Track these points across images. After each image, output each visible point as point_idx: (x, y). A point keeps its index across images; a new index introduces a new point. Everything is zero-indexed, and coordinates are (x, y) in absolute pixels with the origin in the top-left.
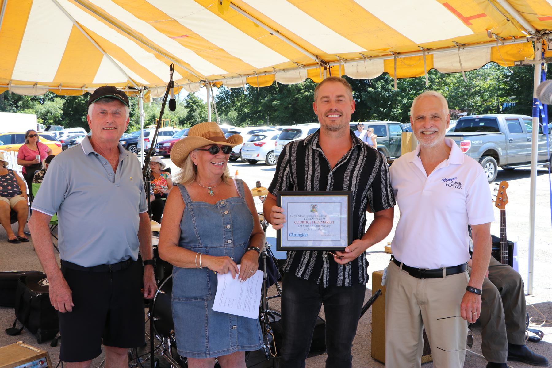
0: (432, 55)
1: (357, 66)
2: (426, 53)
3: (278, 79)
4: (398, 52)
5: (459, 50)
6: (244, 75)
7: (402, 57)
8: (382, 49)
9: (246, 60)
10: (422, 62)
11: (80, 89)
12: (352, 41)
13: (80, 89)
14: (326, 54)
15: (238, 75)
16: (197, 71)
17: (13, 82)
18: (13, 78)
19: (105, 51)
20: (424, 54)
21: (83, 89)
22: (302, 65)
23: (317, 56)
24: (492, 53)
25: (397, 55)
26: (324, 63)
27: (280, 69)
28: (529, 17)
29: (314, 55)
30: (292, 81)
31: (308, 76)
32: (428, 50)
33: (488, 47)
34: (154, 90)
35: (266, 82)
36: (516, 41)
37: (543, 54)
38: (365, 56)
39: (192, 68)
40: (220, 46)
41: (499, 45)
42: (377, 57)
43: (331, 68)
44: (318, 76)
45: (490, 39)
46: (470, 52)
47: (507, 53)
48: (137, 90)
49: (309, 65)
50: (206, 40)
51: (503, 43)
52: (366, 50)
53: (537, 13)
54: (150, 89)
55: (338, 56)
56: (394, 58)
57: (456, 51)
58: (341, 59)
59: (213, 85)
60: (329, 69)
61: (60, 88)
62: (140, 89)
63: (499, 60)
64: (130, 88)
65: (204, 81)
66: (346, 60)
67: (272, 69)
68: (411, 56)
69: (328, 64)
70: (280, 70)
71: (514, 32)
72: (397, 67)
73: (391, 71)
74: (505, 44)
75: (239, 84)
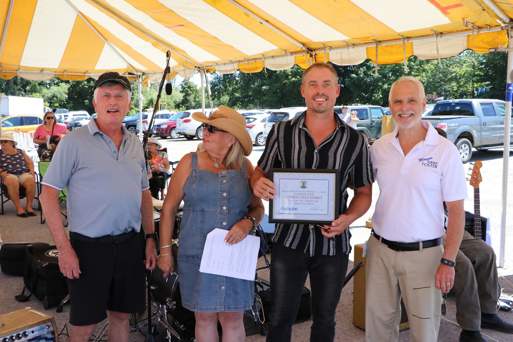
0: (412, 43)
1: (341, 53)
2: (406, 41)
3: (268, 66)
4: (379, 40)
5: (437, 38)
6: (236, 62)
7: (383, 45)
8: (364, 38)
9: (237, 47)
10: (403, 49)
12: (337, 30)
13: (84, 74)
14: (312, 41)
16: (192, 58)
18: (22, 64)
19: (106, 40)
20: (404, 42)
21: (86, 74)
22: (290, 53)
24: (468, 41)
25: (378, 43)
26: (310, 50)
28: (504, 7)
29: (301, 43)
30: (281, 67)
32: (408, 38)
33: (465, 36)
34: (152, 76)
35: (257, 68)
36: (491, 30)
38: (349, 44)
39: (187, 55)
40: (213, 34)
41: (474, 33)
42: (359, 45)
44: (304, 62)
45: (466, 28)
46: (448, 40)
47: (482, 41)
48: (136, 76)
49: (296, 53)
50: (200, 28)
51: (479, 31)
52: (349, 38)
53: (511, 3)
54: (148, 75)
55: (324, 44)
56: (375, 46)
57: (434, 39)
58: (326, 47)
61: (65, 73)
62: (138, 75)
63: (475, 47)
64: (130, 74)
65: (199, 68)
66: (331, 47)
67: (262, 56)
68: (392, 44)
69: (314, 51)
70: (269, 57)
73: (373, 57)
74: (480, 32)
75: (231, 70)
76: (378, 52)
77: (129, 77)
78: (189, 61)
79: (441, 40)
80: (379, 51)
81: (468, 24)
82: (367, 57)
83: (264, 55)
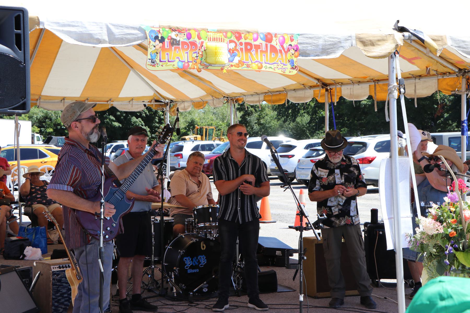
3: (290, 98)
6: (262, 93)
7: (381, 83)
9: (259, 81)
11: (106, 103)
14: (323, 78)
15: (255, 93)
16: (220, 90)
17: (42, 98)
18: (43, 93)
19: (132, 67)
21: (109, 103)
22: (308, 87)
23: (319, 79)
25: (376, 82)
27: (291, 90)
30: (301, 100)
31: (314, 96)
34: (181, 104)
35: (280, 100)
39: (214, 86)
43: (332, 89)
44: (318, 97)
46: (425, 82)
47: (447, 84)
48: (164, 103)
51: (443, 77)
54: (177, 103)
55: (334, 81)
56: (374, 84)
58: (336, 83)
59: (235, 101)
60: (330, 91)
63: (442, 89)
65: (227, 98)
67: (284, 89)
68: (386, 83)
69: (328, 86)
70: (291, 90)
71: (445, 70)
73: (373, 94)
75: (257, 102)
76: (377, 90)
77: (155, 104)
78: (217, 91)
80: (378, 88)
81: (431, 70)
82: (370, 93)
83: (285, 89)
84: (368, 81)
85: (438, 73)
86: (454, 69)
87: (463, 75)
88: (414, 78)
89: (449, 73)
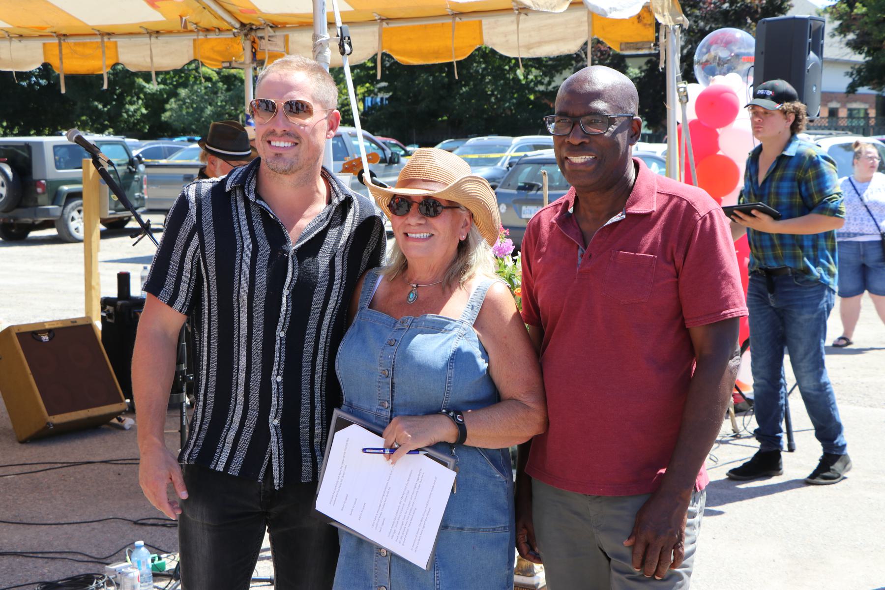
0: (116, 42)
2: (106, 39)
4: (63, 32)
5: (150, 39)
7: (71, 41)
10: (99, 52)
20: (103, 41)
32: (110, 34)
37: (254, 54)
41: (200, 37)
45: (186, 30)
47: (212, 49)
51: (206, 35)
53: (235, 3)
56: (57, 41)
57: (146, 40)
63: (204, 58)
68: (85, 41)
71: (215, 23)
72: (64, 57)
73: (55, 62)
74: (208, 37)
79: (158, 44)
81: (188, 24)
84: (41, 36)
85: (198, 28)
86: (233, 22)
87: (246, 35)
88: (148, 35)
89: (219, 29)
